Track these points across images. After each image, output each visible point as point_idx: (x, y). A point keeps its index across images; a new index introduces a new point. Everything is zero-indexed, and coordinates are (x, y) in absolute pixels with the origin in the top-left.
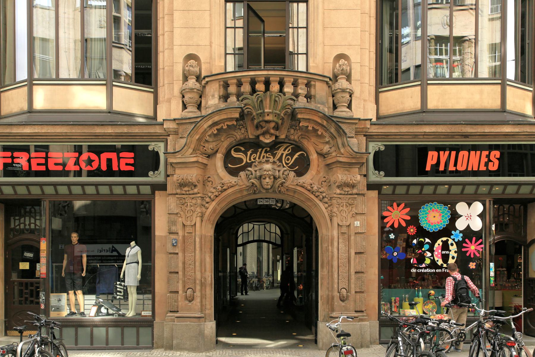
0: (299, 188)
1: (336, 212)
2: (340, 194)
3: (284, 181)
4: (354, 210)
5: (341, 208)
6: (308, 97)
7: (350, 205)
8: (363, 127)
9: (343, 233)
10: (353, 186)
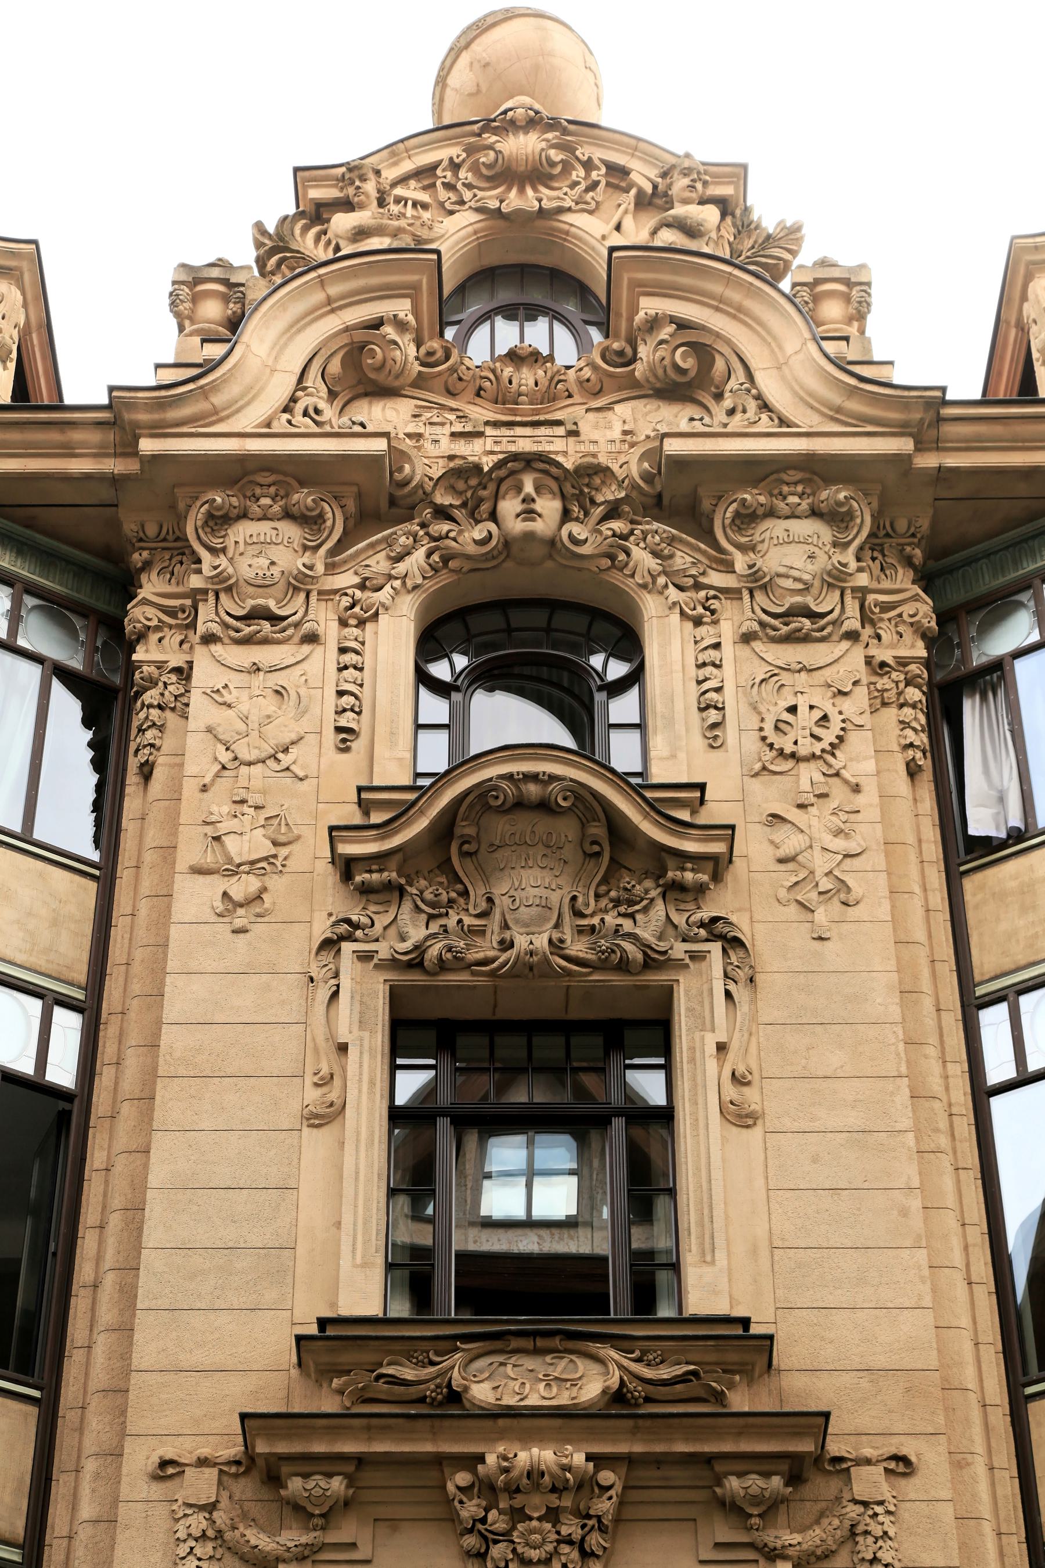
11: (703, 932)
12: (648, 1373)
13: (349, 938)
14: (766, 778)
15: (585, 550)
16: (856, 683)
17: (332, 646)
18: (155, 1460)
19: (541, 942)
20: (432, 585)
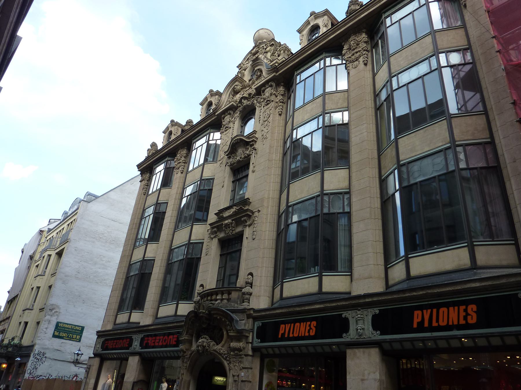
0: (214, 352)
1: (232, 367)
2: (234, 355)
3: (207, 348)
4: (242, 365)
5: (235, 364)
6: (229, 300)
7: (240, 362)
8: (249, 313)
9: (235, 381)
10: (240, 350)
11: (253, 149)
12: (237, 208)
13: (227, 164)
14: (263, 125)
15: (250, 104)
16: (272, 107)
17: (232, 128)
18: (207, 230)
19: (239, 158)
20: (240, 115)
